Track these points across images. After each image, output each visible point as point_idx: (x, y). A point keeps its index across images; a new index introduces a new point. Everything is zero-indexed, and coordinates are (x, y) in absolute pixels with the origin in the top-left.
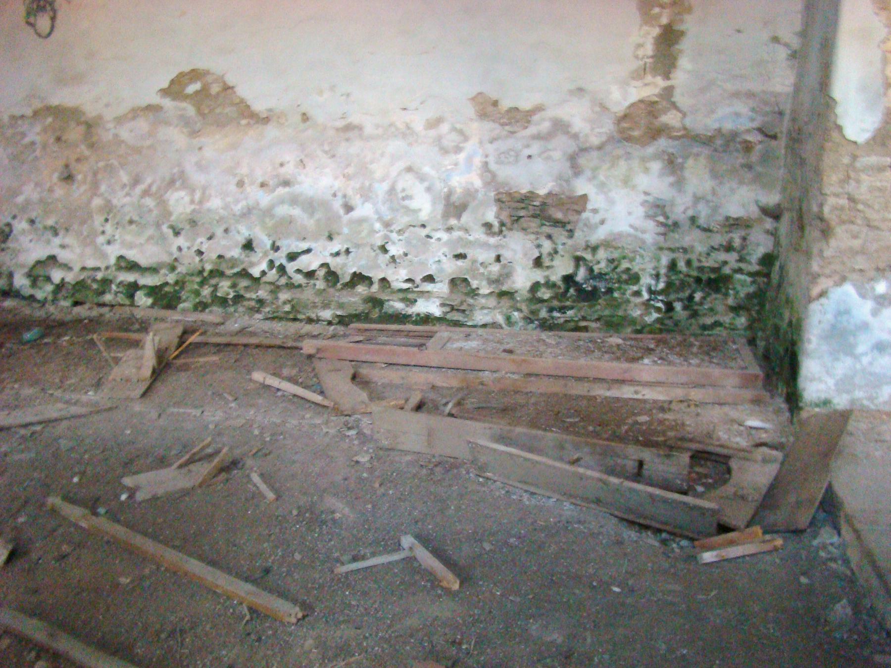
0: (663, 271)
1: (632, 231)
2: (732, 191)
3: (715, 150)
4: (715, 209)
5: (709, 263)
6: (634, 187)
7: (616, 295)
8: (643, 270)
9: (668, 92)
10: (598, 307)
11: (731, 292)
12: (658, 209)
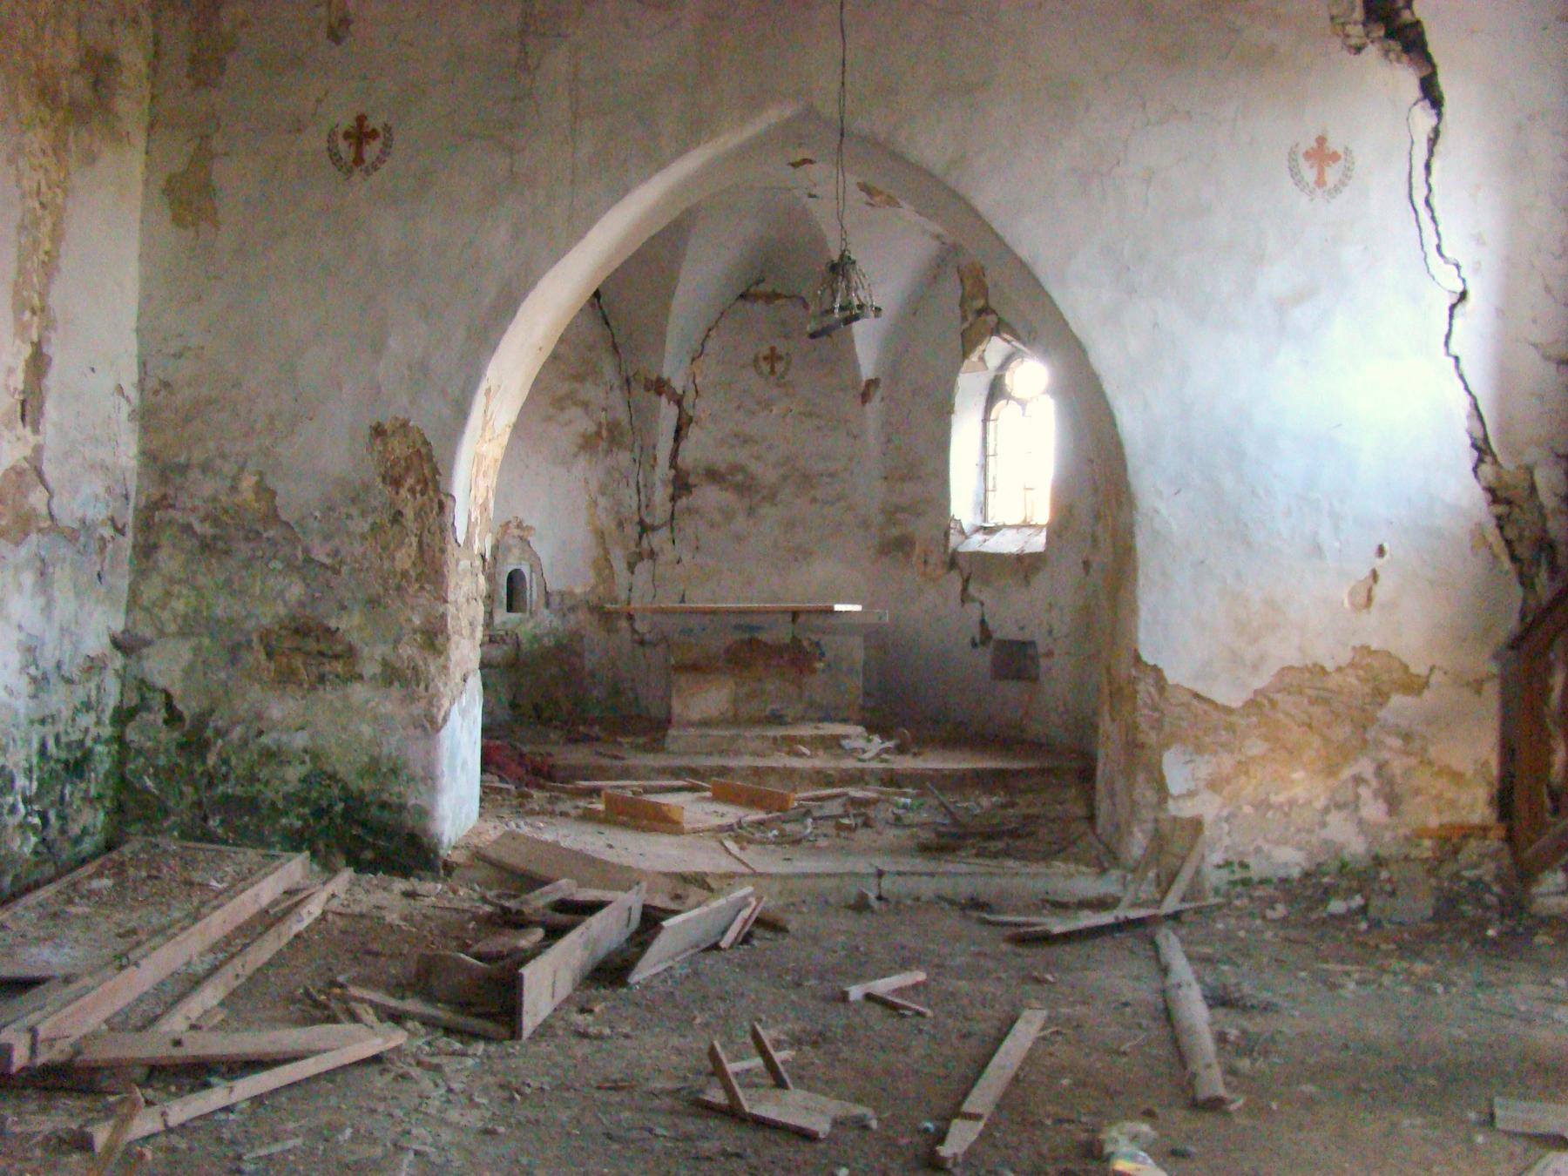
0: (35, 760)
2: (91, 615)
4: (76, 648)
5: (76, 736)
8: (16, 765)
9: (38, 450)
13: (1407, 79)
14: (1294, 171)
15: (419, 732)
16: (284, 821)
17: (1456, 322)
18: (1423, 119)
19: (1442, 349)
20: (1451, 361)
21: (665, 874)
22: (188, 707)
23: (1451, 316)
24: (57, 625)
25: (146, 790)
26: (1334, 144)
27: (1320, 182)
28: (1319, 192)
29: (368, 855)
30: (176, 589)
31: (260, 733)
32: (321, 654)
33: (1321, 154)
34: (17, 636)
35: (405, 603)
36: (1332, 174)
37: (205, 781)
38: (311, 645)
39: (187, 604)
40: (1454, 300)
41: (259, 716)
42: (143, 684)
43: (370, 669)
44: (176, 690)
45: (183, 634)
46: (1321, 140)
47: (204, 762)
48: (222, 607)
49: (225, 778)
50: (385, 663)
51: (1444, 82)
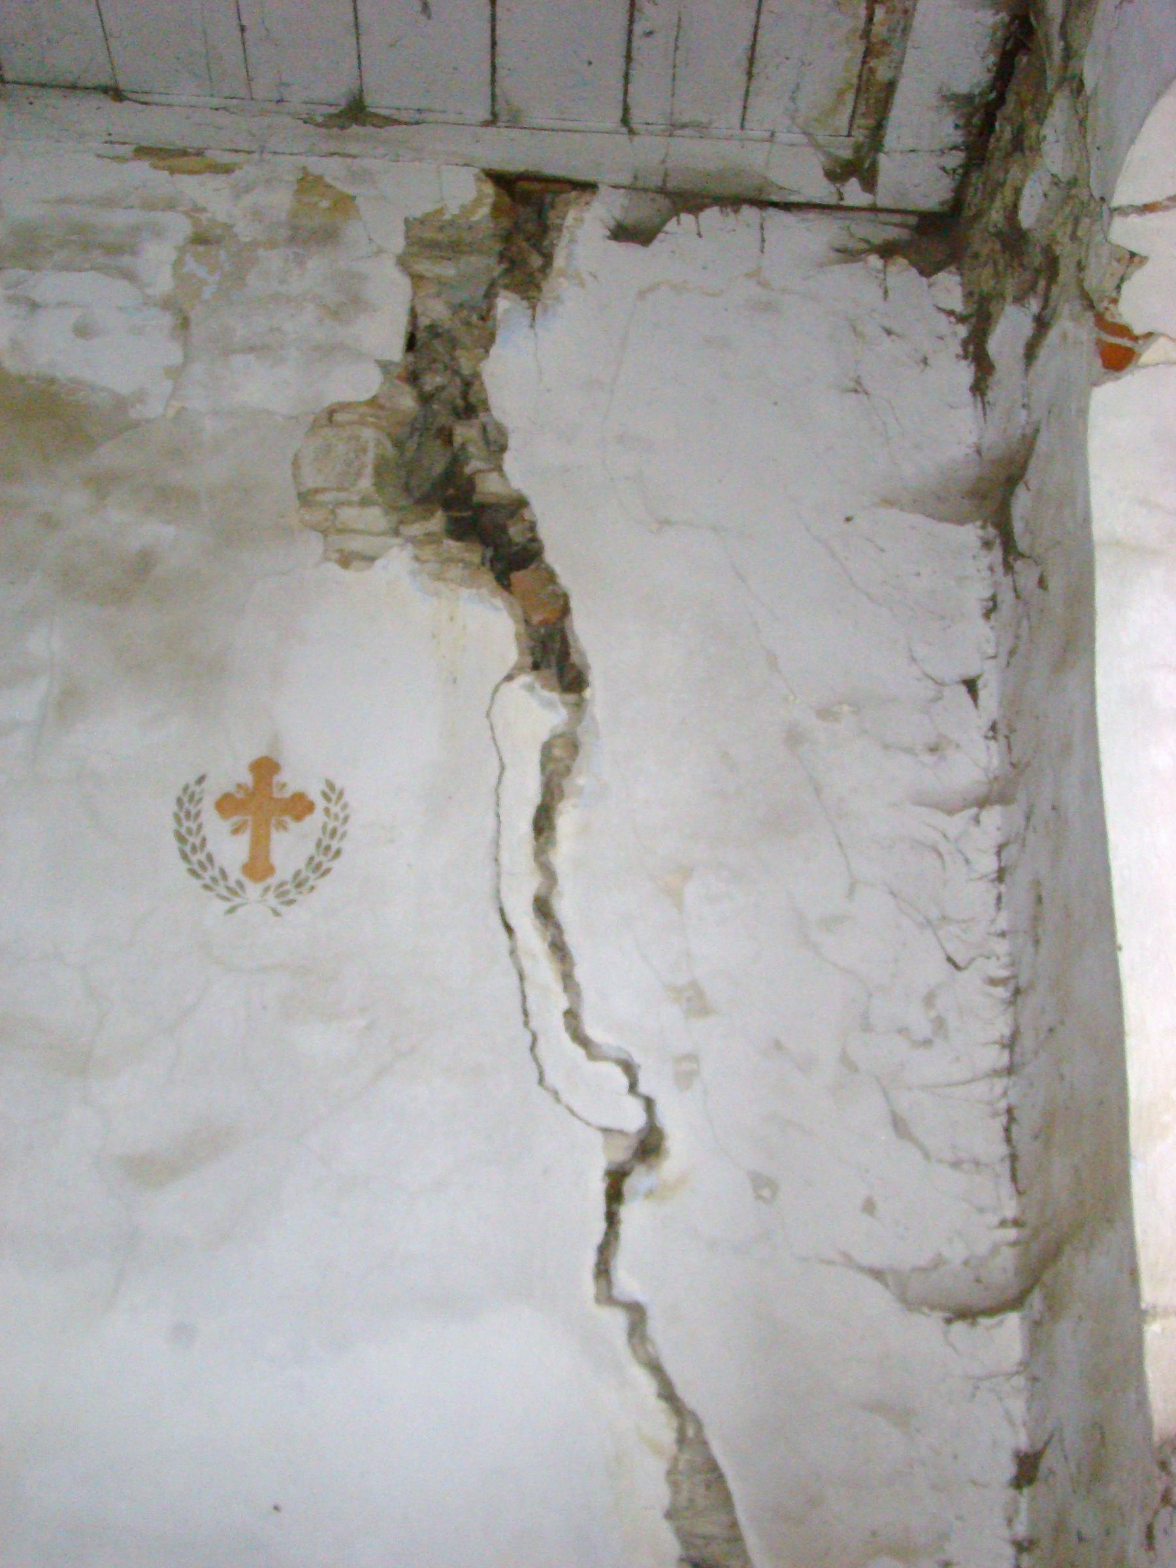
13: (490, 625)
14: (190, 845)
17: (629, 1213)
18: (535, 713)
19: (588, 1286)
20: (616, 1321)
23: (615, 1195)
26: (295, 778)
27: (258, 866)
28: (253, 890)
33: (264, 799)
36: (290, 847)
40: (622, 1153)
46: (265, 768)
51: (587, 632)
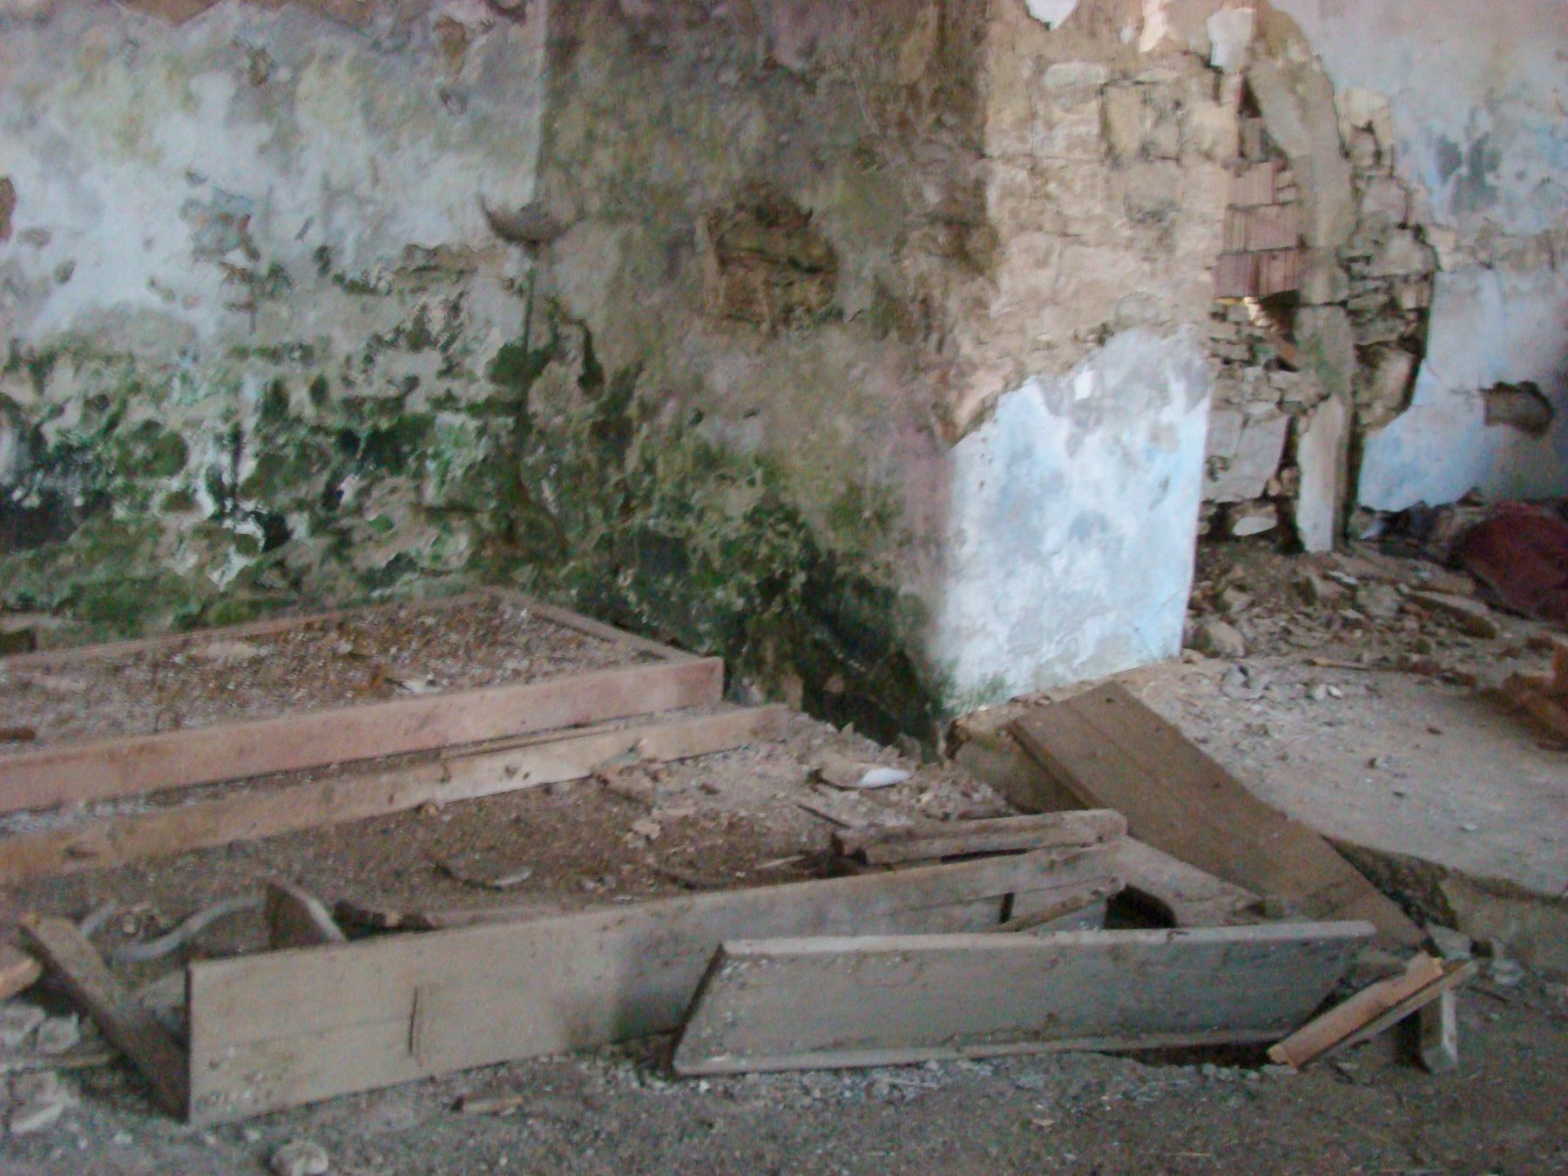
0: (250, 423)
1: (155, 301)
2: (422, 169)
3: (376, 45)
4: (379, 225)
5: (373, 387)
6: (154, 158)
7: (120, 512)
8: (194, 424)
10: (66, 560)
11: (431, 466)
12: (228, 225)
15: (920, 441)
16: (719, 594)
21: (1326, 839)
22: (611, 360)
24: (312, 178)
25: (542, 508)
29: (835, 685)
30: (601, 127)
31: (699, 417)
32: (794, 263)
34: (181, 191)
35: (912, 158)
37: (620, 500)
38: (780, 244)
39: (615, 157)
41: (698, 385)
42: (556, 312)
43: (856, 299)
44: (597, 324)
45: (611, 217)
47: (621, 466)
48: (664, 165)
49: (647, 500)
50: (882, 291)
